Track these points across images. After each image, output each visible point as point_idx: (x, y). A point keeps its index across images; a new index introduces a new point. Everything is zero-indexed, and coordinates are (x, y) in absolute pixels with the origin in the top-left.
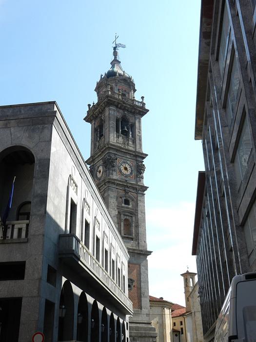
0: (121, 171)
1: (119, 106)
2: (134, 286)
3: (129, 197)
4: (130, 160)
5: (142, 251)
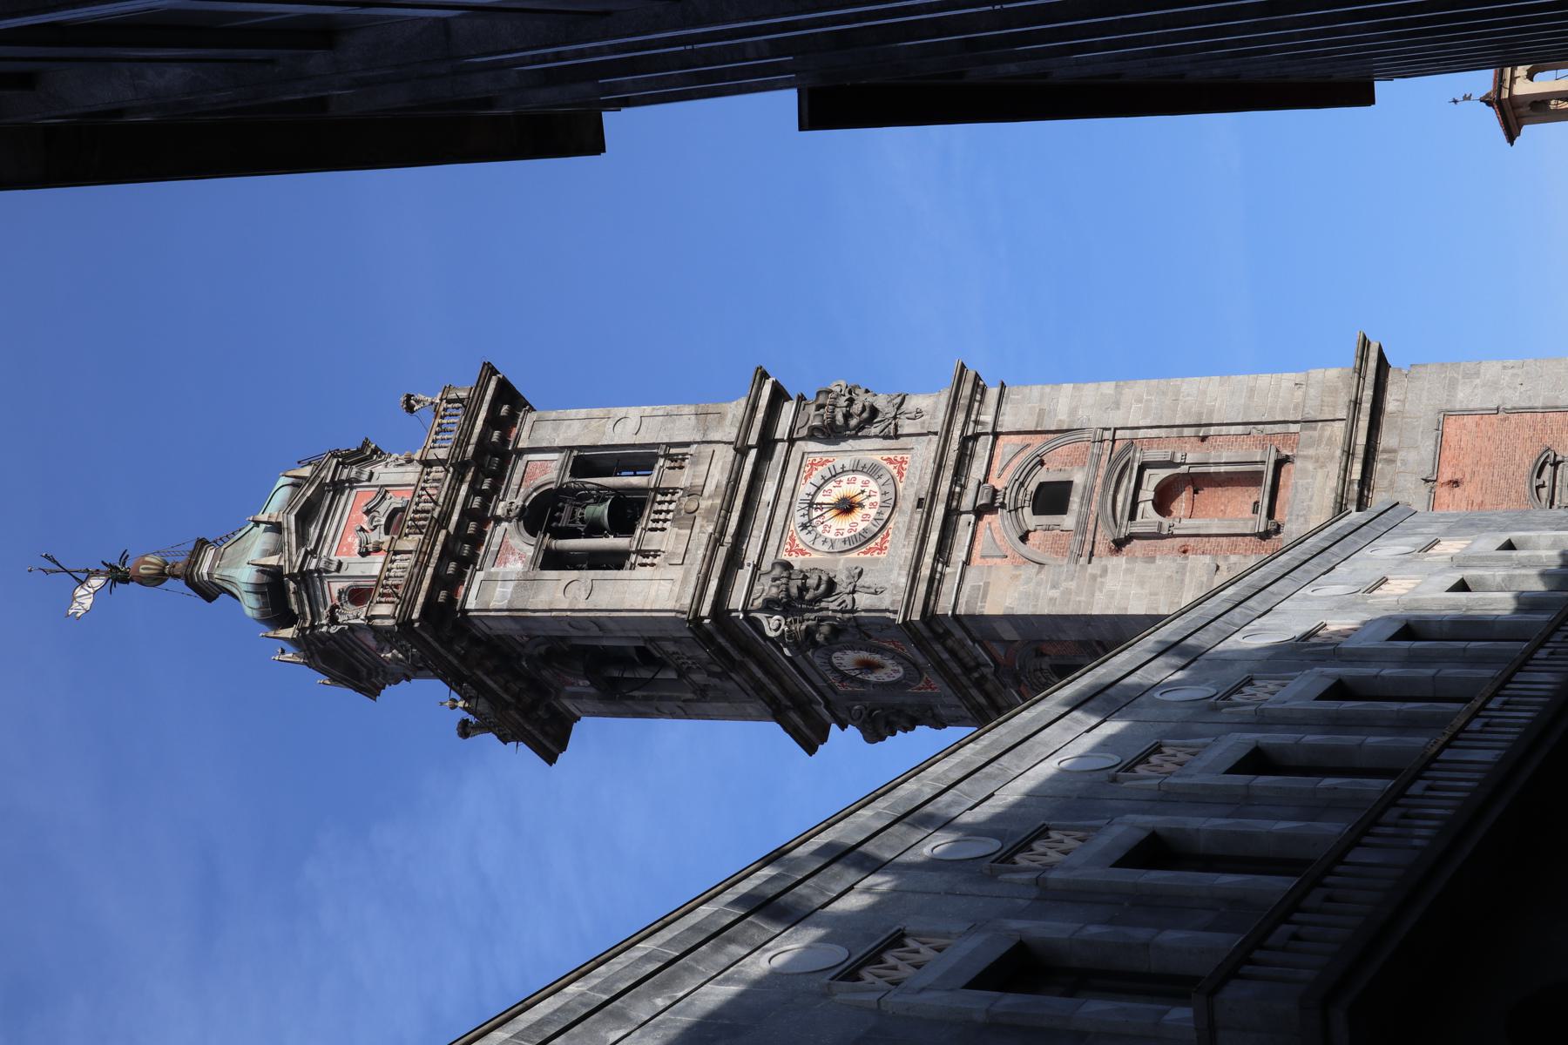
0: (862, 541)
4: (789, 483)
5: (1356, 404)
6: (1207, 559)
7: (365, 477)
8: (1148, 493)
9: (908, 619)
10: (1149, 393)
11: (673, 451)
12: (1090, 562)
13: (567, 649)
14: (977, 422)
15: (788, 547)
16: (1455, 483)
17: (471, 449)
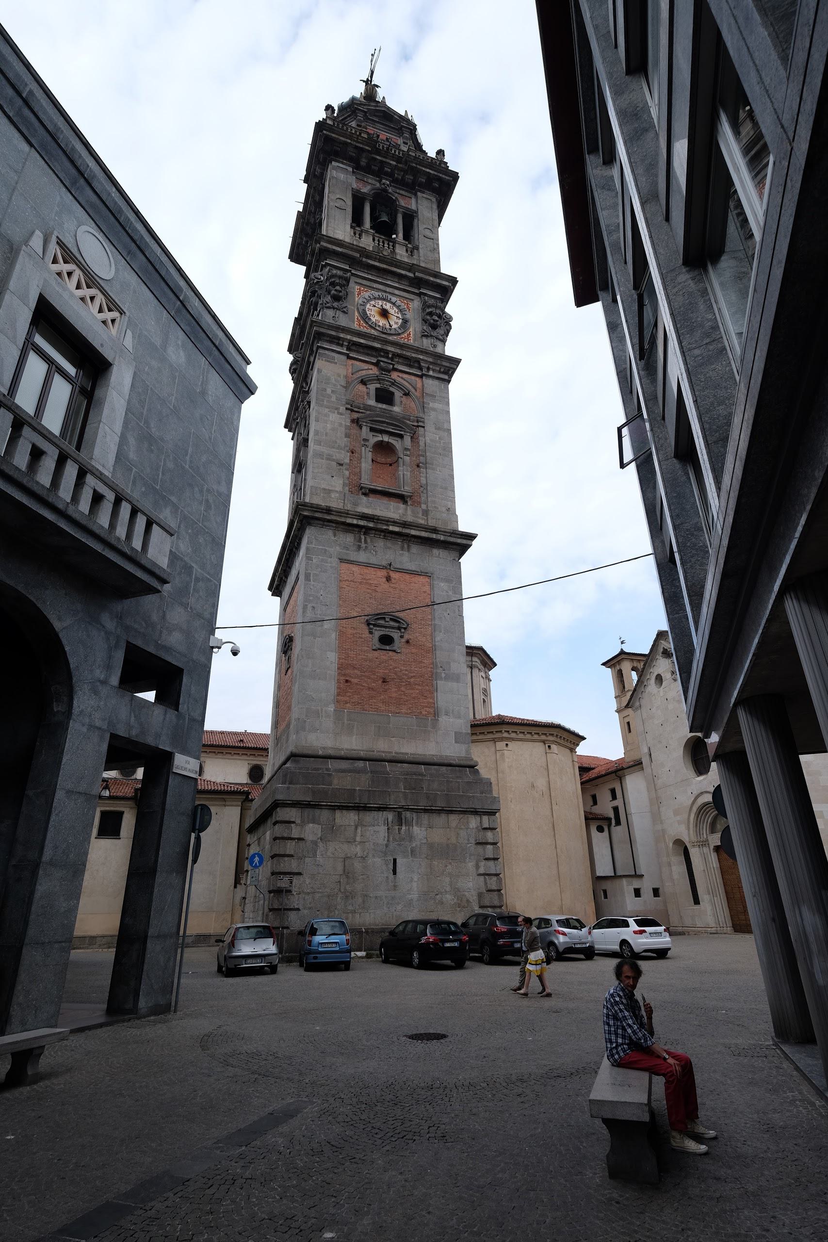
0: (365, 317)
1: (364, 162)
2: (408, 642)
3: (394, 383)
4: (397, 292)
5: (435, 530)
6: (347, 461)
8: (386, 438)
10: (444, 443)
12: (347, 409)
14: (428, 369)
16: (388, 579)
17: (414, 165)
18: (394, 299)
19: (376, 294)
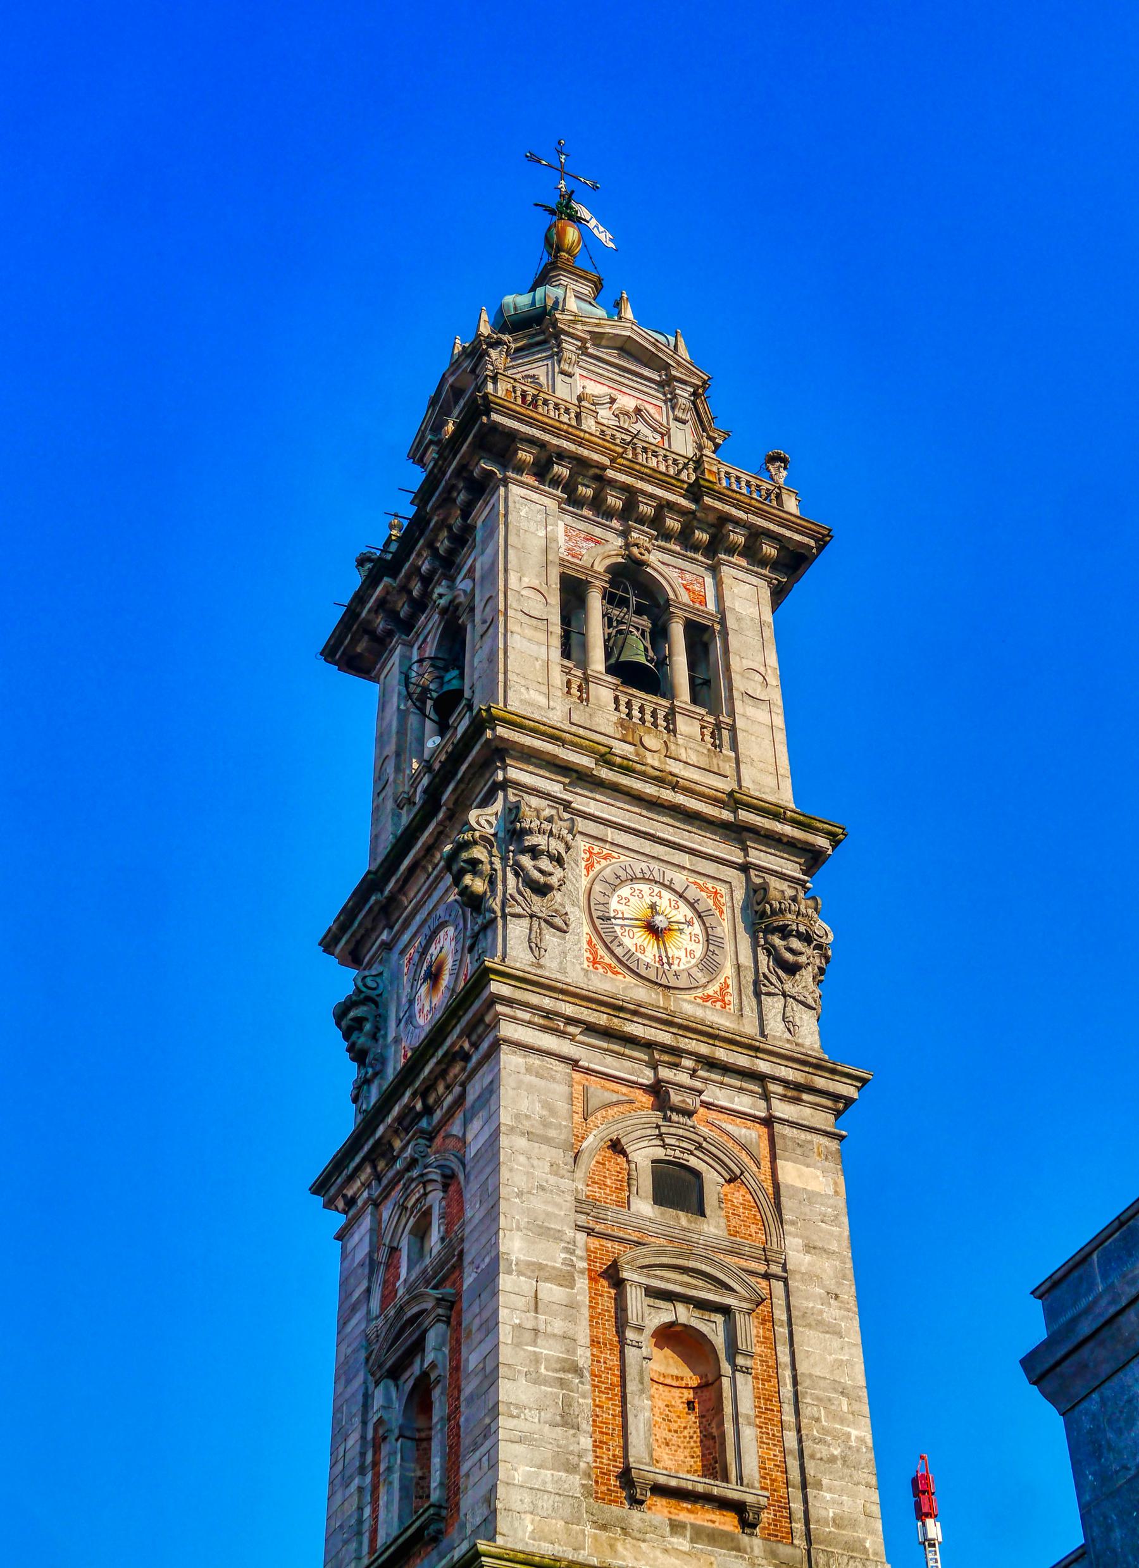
7: (680, 415)
8: (684, 1314)
9: (492, 976)
11: (725, 733)
12: (579, 1228)
13: (460, 621)
15: (596, 850)
18: (680, 879)
19: (640, 866)
